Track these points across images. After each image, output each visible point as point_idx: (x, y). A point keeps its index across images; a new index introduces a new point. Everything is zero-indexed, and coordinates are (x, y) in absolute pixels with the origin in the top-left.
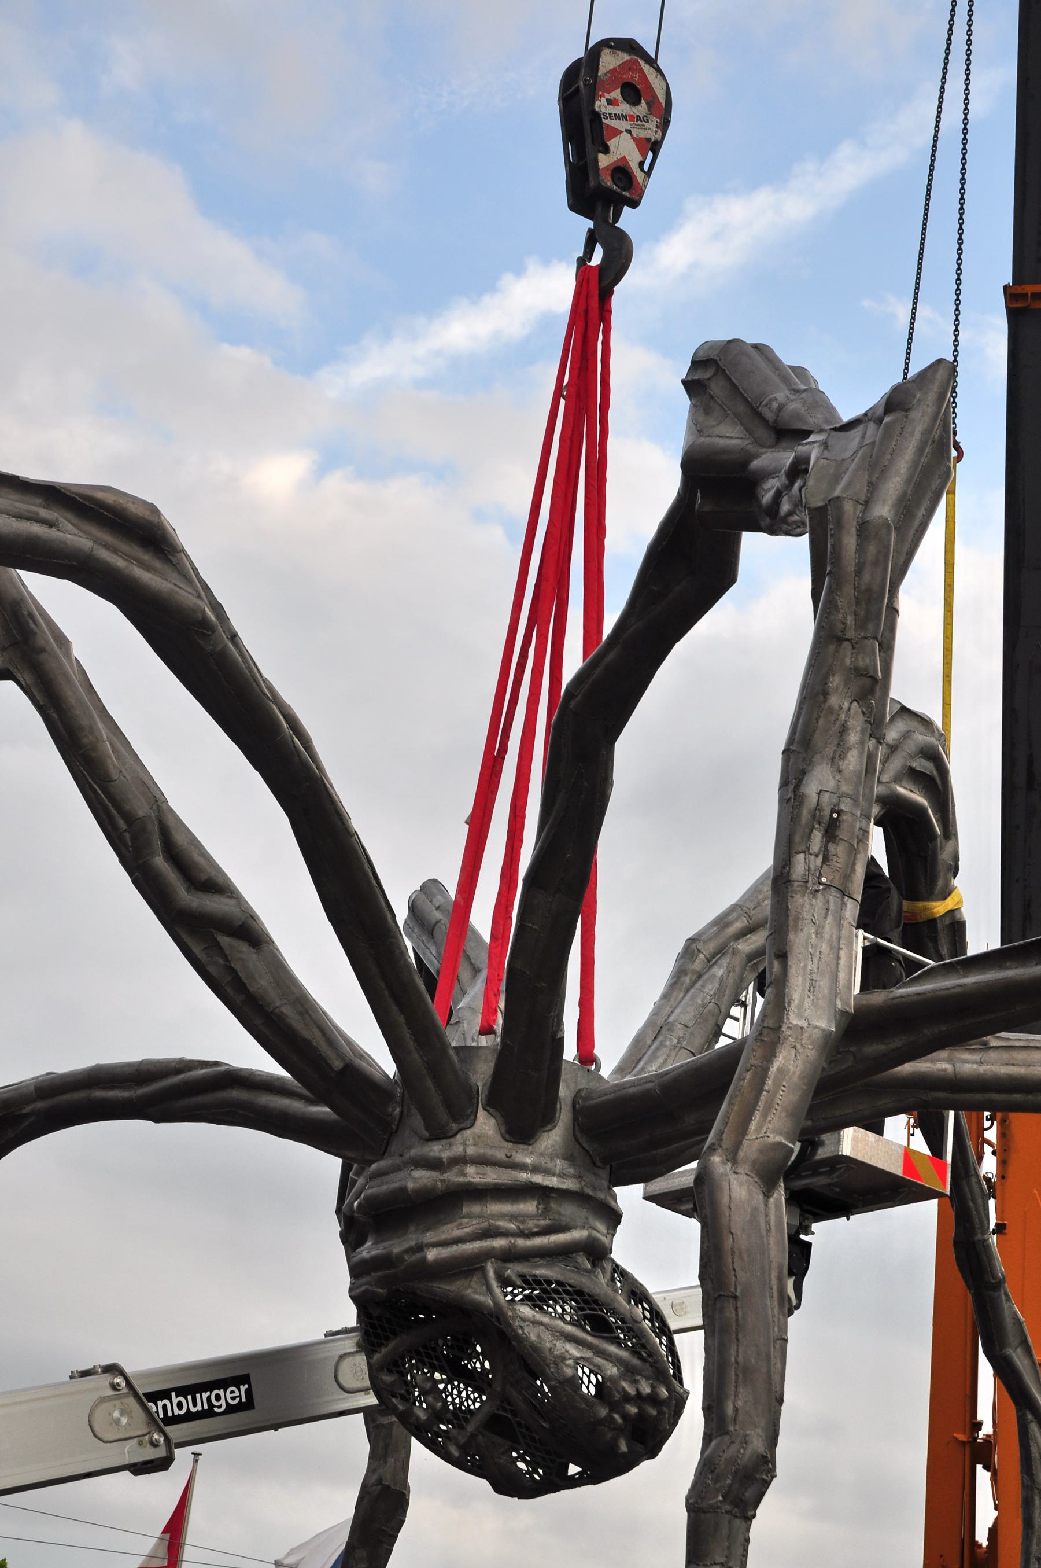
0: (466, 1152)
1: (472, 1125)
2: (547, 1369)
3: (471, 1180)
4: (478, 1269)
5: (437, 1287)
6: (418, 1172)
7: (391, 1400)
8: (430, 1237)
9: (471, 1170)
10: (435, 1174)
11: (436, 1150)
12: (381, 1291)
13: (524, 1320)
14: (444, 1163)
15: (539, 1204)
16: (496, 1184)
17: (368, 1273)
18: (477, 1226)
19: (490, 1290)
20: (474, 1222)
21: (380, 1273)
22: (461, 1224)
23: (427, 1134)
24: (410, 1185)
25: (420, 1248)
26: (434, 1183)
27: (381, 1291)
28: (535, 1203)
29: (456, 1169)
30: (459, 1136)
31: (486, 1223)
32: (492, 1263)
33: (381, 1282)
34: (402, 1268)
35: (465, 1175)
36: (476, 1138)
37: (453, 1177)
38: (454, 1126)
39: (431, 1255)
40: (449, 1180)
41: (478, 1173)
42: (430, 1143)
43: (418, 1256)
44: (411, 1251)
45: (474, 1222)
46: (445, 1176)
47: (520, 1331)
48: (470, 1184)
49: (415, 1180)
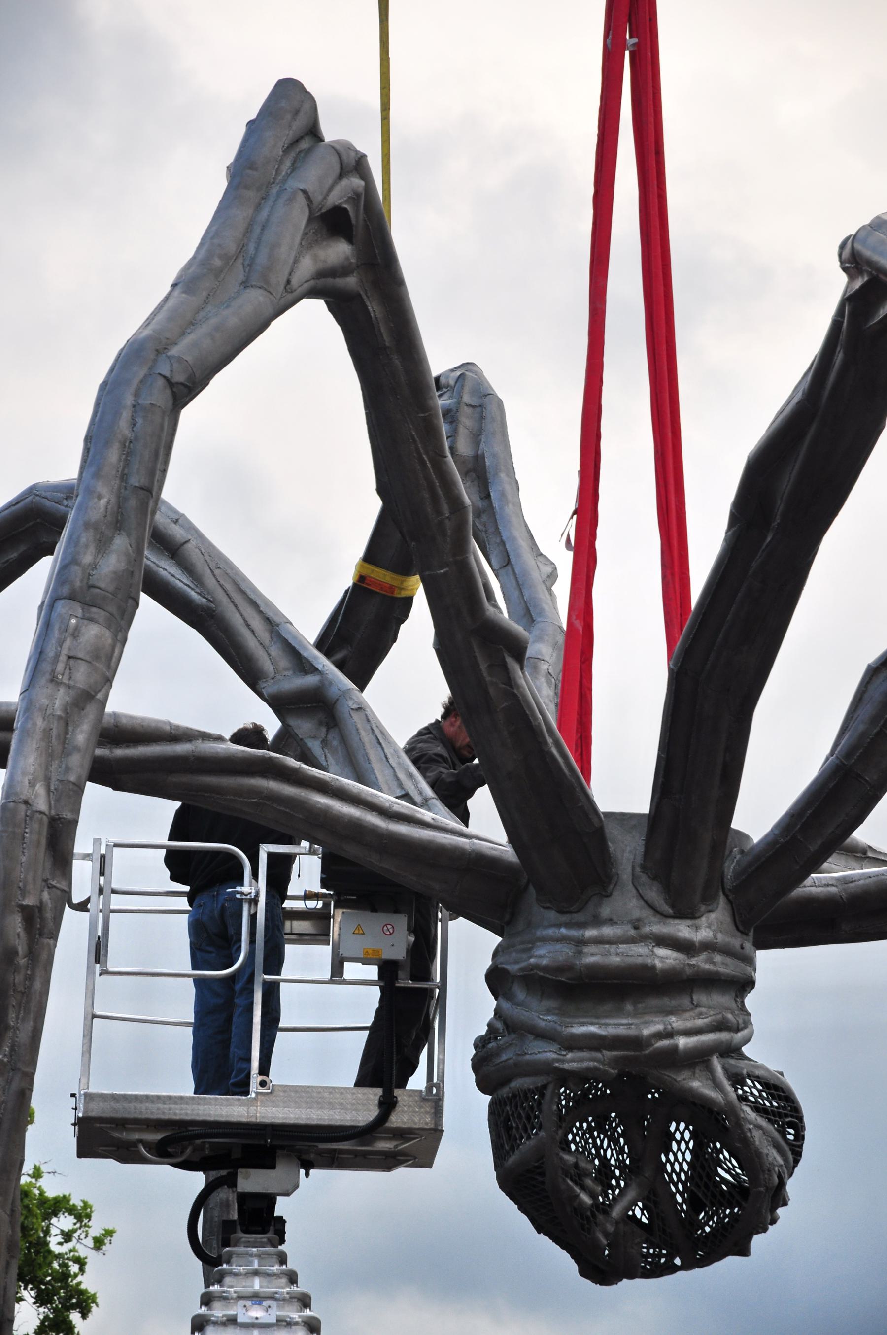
0: (716, 939)
1: (717, 908)
2: (762, 1177)
3: (719, 969)
4: (703, 1062)
5: (668, 1076)
6: (661, 950)
7: (564, 1181)
8: (676, 1022)
9: (718, 958)
10: (681, 956)
11: (683, 930)
12: (612, 1071)
13: (750, 1123)
14: (696, 947)
15: (737, 996)
16: (734, 977)
17: (597, 1049)
18: (713, 1018)
19: (717, 1086)
20: (712, 1013)
21: (615, 1053)
22: (701, 1014)
23: (670, 911)
24: (658, 964)
25: (669, 1034)
26: (682, 966)
27: (612, 1071)
28: (734, 995)
29: (703, 956)
30: (704, 919)
31: (720, 1016)
32: (717, 1057)
33: (615, 1062)
34: (647, 1052)
35: (714, 963)
36: (720, 923)
37: (701, 962)
38: (703, 908)
39: (682, 1042)
40: (698, 966)
41: (723, 963)
42: (671, 921)
43: (665, 1043)
44: (660, 1036)
45: (712, 1013)
46: (693, 961)
47: (749, 1134)
48: (717, 973)
49: (662, 958)
